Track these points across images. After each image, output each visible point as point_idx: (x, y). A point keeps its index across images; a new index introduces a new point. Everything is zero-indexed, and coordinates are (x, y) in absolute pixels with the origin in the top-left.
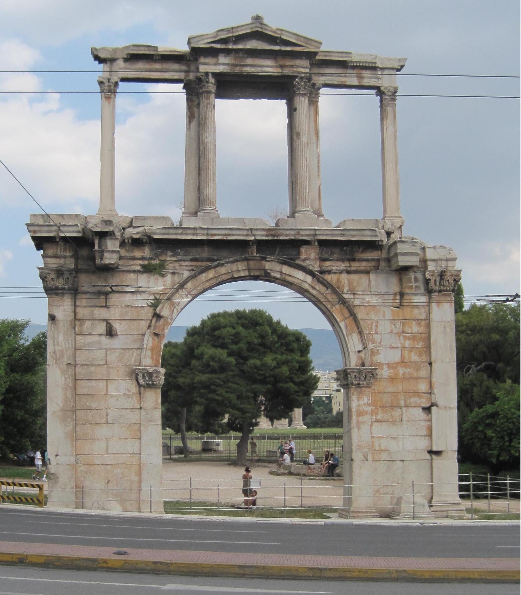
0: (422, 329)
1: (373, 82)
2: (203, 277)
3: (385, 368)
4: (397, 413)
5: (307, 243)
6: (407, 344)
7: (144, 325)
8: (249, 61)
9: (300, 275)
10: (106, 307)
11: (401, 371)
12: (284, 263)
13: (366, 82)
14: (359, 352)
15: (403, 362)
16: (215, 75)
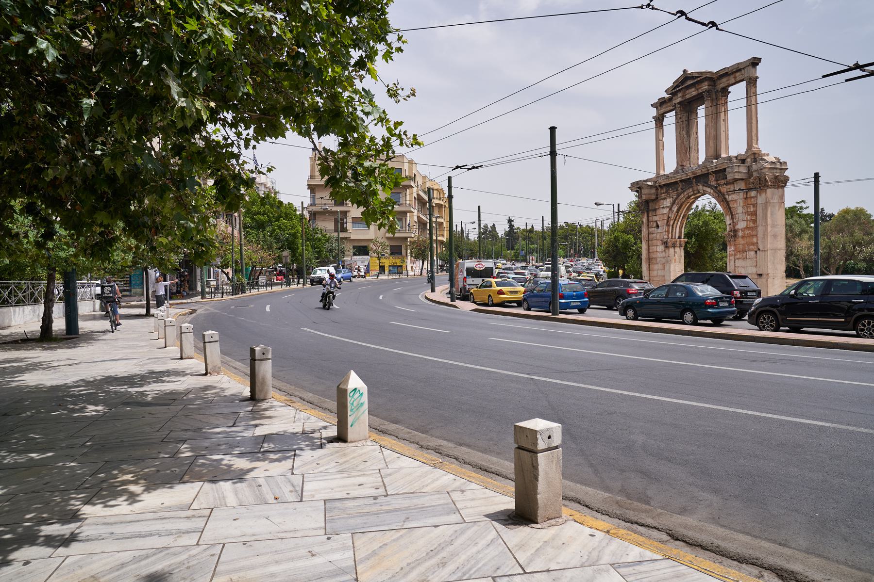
0: (755, 209)
1: (741, 77)
2: (680, 197)
3: (740, 231)
4: (744, 254)
5: (708, 174)
6: (749, 218)
7: (666, 221)
8: (687, 92)
9: (709, 190)
10: (656, 215)
11: (747, 232)
12: (703, 186)
13: (738, 79)
14: (730, 224)
15: (747, 228)
16: (678, 103)
